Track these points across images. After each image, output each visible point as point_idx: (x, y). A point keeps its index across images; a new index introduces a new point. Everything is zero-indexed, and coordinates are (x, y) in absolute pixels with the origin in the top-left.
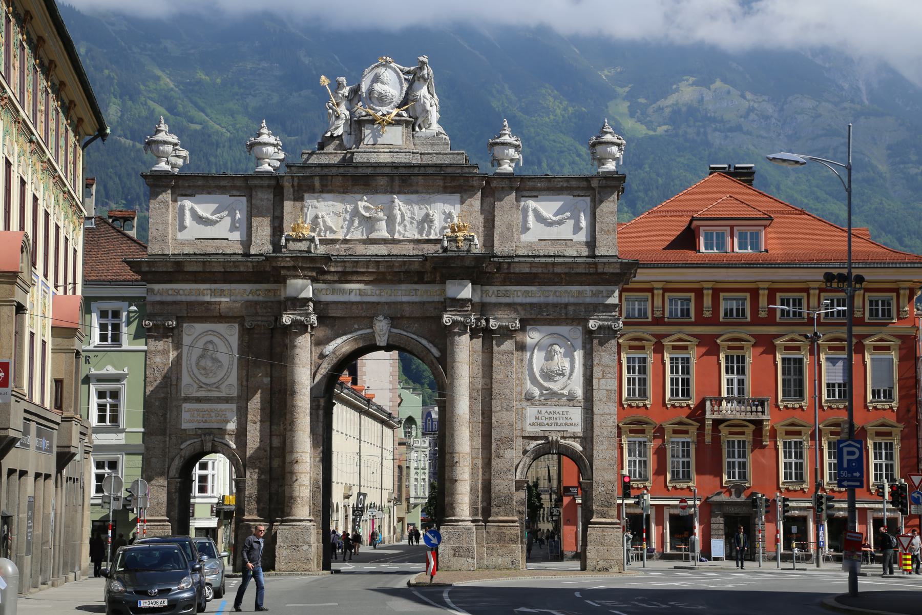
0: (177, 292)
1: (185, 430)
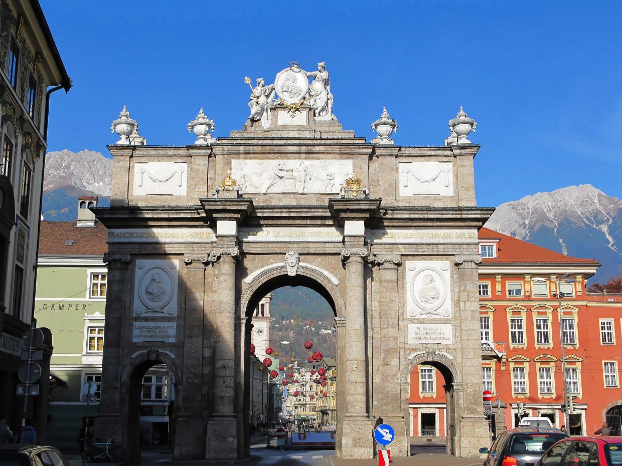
0: (132, 235)
1: (135, 343)
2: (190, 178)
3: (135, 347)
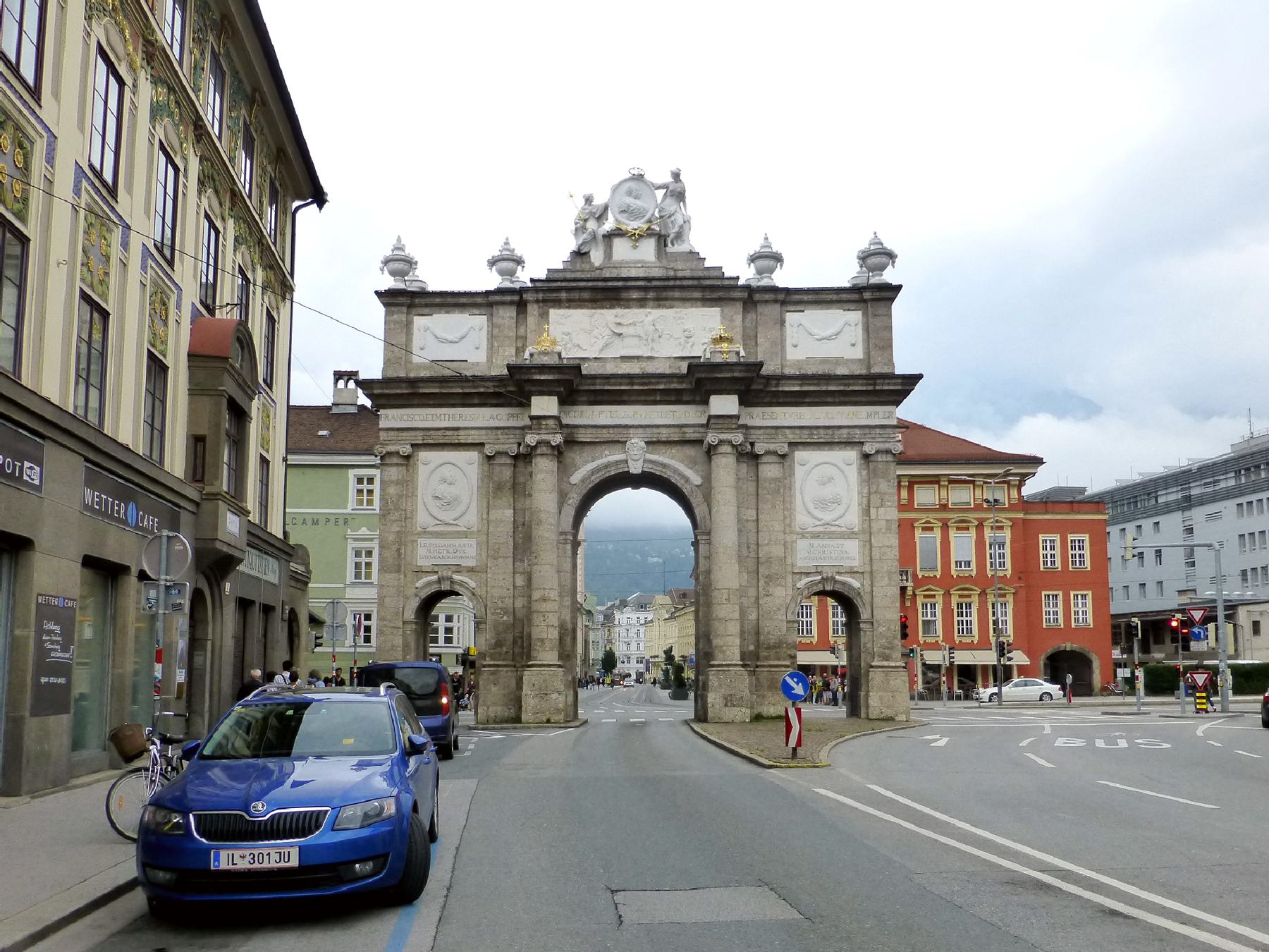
2: (491, 337)
3: (420, 572)
